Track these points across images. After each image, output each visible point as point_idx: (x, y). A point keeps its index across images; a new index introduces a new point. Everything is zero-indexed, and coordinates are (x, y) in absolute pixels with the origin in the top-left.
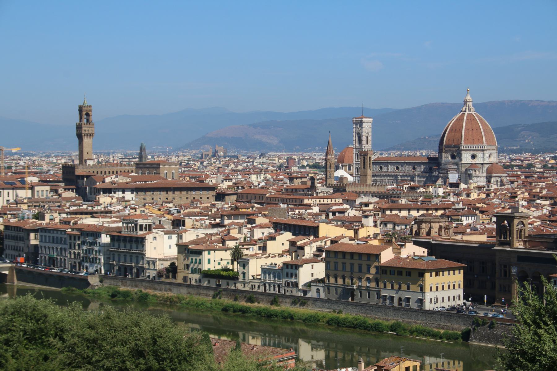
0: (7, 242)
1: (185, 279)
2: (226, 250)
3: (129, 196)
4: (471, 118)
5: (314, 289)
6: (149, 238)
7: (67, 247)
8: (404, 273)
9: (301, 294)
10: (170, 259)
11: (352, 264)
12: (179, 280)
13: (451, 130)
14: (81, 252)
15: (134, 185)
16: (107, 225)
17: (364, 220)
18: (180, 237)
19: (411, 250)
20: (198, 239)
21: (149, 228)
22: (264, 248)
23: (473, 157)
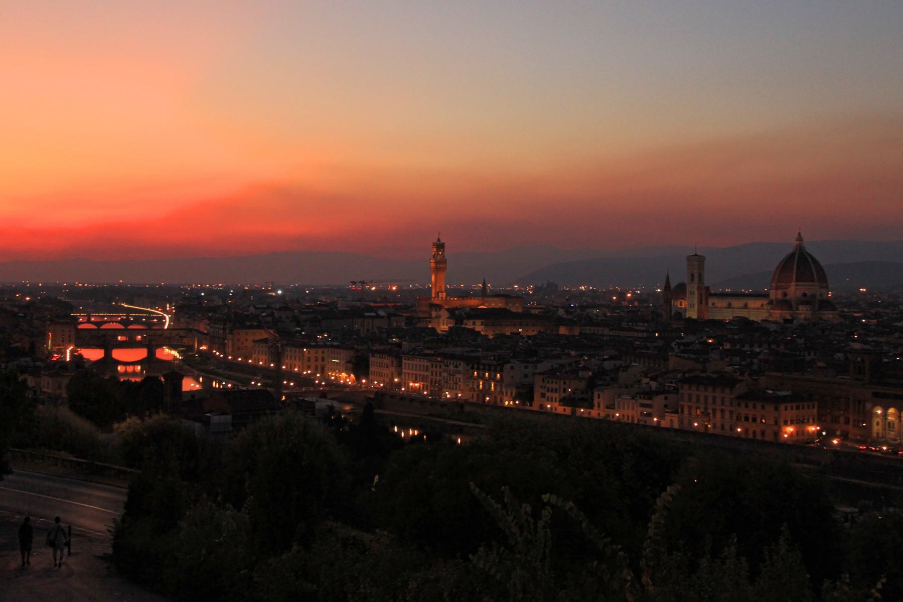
0: (372, 369)
1: (541, 406)
5: (668, 417)
6: (507, 367)
7: (429, 374)
11: (706, 397)
22: (614, 380)
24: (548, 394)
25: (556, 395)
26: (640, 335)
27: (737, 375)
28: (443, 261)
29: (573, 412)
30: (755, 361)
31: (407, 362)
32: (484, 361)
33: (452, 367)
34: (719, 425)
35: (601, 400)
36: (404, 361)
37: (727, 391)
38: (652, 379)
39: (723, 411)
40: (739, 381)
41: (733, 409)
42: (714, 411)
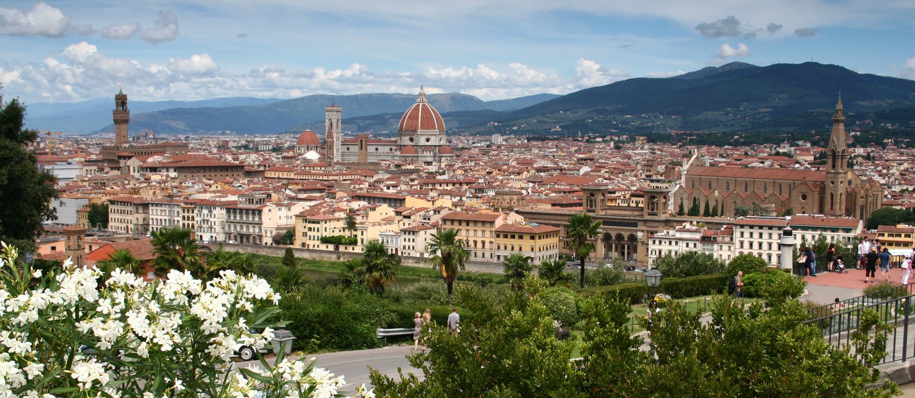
0: (111, 216)
1: (303, 245)
2: (338, 220)
3: (173, 174)
4: (425, 109)
6: (265, 210)
8: (517, 236)
9: (418, 255)
10: (285, 228)
12: (297, 245)
13: (409, 117)
14: (195, 222)
15: (176, 165)
16: (218, 199)
17: (433, 194)
18: (289, 210)
19: (514, 218)
20: (306, 211)
21: (261, 201)
23: (428, 140)
24: (309, 233)
25: (315, 234)
26: (325, 178)
27: (490, 212)
28: (126, 111)
29: (337, 248)
30: (464, 199)
31: (155, 208)
32: (240, 206)
33: (205, 211)
34: (480, 254)
35: (364, 237)
36: (151, 208)
37: (488, 225)
38: (405, 217)
39: (483, 243)
40: (497, 216)
41: (493, 240)
42: (475, 242)
